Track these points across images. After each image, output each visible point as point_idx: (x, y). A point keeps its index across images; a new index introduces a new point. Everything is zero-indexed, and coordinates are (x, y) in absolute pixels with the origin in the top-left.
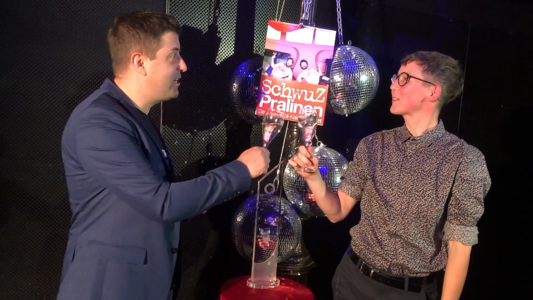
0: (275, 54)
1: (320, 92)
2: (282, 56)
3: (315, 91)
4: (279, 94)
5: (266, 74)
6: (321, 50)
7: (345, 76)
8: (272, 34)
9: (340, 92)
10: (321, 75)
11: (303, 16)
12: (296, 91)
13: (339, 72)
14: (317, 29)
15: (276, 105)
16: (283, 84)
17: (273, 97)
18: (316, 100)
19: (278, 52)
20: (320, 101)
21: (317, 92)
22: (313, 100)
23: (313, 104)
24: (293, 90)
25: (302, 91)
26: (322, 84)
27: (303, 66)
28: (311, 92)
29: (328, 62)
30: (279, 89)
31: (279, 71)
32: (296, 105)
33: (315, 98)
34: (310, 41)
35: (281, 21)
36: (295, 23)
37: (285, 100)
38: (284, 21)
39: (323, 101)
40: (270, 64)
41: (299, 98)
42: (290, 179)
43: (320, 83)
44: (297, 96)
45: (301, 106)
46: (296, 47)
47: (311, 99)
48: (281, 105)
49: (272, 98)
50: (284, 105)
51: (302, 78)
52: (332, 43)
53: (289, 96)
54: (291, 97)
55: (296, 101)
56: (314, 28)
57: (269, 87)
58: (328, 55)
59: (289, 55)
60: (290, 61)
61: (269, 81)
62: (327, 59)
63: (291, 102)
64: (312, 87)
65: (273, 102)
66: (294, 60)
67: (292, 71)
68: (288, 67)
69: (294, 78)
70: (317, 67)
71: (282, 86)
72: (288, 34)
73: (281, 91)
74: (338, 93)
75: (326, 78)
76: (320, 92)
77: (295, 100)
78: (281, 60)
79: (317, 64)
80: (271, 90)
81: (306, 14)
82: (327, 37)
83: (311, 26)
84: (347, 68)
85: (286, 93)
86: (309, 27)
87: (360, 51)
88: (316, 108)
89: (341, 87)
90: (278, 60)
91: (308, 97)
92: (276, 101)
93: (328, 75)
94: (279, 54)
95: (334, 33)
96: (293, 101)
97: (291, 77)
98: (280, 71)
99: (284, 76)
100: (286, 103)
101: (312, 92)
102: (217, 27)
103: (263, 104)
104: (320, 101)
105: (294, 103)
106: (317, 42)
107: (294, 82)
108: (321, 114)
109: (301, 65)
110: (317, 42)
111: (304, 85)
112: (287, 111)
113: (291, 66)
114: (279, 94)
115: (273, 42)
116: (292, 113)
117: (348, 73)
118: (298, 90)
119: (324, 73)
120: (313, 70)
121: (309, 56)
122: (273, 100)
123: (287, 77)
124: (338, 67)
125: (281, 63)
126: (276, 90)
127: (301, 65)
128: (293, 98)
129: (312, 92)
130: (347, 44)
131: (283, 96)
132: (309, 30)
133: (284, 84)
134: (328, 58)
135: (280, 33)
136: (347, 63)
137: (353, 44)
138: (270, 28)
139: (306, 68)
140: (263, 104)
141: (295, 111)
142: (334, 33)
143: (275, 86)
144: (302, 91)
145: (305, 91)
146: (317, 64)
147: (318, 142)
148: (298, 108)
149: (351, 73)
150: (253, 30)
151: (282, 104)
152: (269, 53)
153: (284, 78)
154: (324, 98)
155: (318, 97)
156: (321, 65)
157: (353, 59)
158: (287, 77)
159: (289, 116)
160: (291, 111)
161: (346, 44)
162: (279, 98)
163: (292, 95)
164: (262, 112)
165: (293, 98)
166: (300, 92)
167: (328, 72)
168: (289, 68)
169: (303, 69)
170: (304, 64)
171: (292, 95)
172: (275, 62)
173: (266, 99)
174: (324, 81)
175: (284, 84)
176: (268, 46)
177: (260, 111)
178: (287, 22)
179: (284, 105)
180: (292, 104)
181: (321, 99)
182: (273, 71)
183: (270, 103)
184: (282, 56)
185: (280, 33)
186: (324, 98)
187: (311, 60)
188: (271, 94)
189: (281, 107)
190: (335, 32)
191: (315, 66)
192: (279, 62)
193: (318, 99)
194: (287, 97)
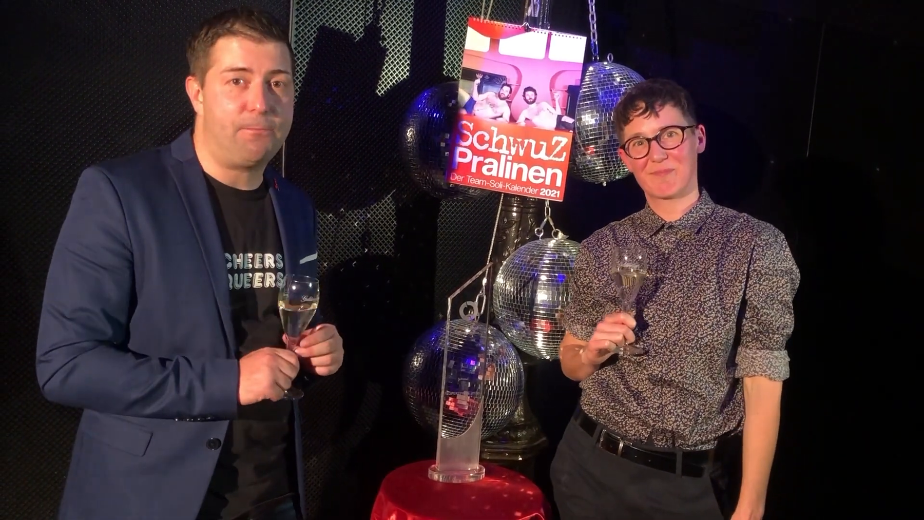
0: (480, 76)
1: (558, 143)
2: (492, 80)
3: (549, 142)
4: (485, 146)
5: (464, 112)
6: (562, 68)
7: (601, 116)
8: (475, 41)
9: (592, 144)
10: (560, 114)
11: (529, 11)
12: (515, 141)
13: (591, 108)
14: (554, 33)
15: (480, 165)
16: (493, 128)
17: (476, 152)
18: (551, 158)
19: (484, 74)
20: (557, 159)
22: (546, 158)
23: (545, 165)
24: (511, 139)
25: (526, 141)
27: (527, 98)
28: (541, 143)
29: (573, 91)
30: (487, 138)
31: (486, 107)
32: (516, 166)
33: (548, 153)
34: (541, 55)
35: (491, 19)
36: (515, 23)
37: (497, 156)
38: (497, 20)
39: (562, 159)
40: (471, 94)
41: (521, 153)
42: (505, 295)
43: (557, 128)
45: (524, 167)
46: (516, 63)
47: (542, 155)
48: (490, 166)
52: (580, 58)
53: (504, 150)
54: (507, 152)
55: (517, 159)
56: (547, 32)
57: (468, 133)
59: (504, 78)
60: (506, 89)
62: (570, 87)
63: (507, 160)
64: (545, 135)
65: (476, 159)
66: (513, 87)
68: (502, 99)
69: (513, 119)
70: (554, 100)
71: (491, 134)
72: (502, 41)
73: (490, 142)
74: (588, 145)
75: (567, 119)
76: (558, 143)
78: (490, 87)
80: (473, 140)
81: (535, 6)
82: (571, 47)
83: (543, 27)
84: (604, 102)
85: (499, 145)
86: (540, 30)
87: (628, 71)
88: (550, 171)
89: (595, 134)
91: (537, 151)
92: (481, 159)
93: (571, 114)
94: (487, 77)
95: (582, 41)
96: (510, 158)
97: (507, 116)
100: (499, 161)
101: (545, 144)
102: (379, 30)
104: (557, 159)
105: (512, 162)
106: (553, 56)
107: (512, 125)
108: (559, 183)
109: (524, 96)
110: (553, 56)
111: (531, 130)
112: (501, 175)
114: (485, 146)
115: (477, 55)
117: (607, 110)
118: (519, 140)
119: (566, 110)
120: (546, 105)
122: (475, 157)
123: (501, 116)
124: (589, 99)
125: (490, 93)
126: (481, 140)
127: (524, 96)
128: (510, 154)
129: (545, 144)
131: (493, 149)
132: (538, 36)
133: (495, 129)
134: (573, 84)
135: (488, 40)
136: (606, 93)
137: (614, 61)
138: (471, 32)
139: (534, 102)
141: (514, 177)
142: (582, 41)
144: (526, 141)
145: (532, 141)
146: (552, 95)
147: (554, 230)
148: (520, 171)
150: (443, 34)
151: (491, 163)
152: (470, 75)
153: (495, 118)
154: (565, 154)
155: (555, 152)
156: (559, 96)
157: (616, 87)
158: (501, 116)
160: (507, 176)
161: (603, 59)
162: (486, 154)
163: (508, 148)
164: (457, 177)
165: (510, 154)
167: (572, 108)
168: (504, 102)
170: (530, 94)
172: (480, 91)
173: (463, 155)
175: (495, 129)
176: (467, 63)
177: (454, 176)
178: (501, 21)
180: (509, 164)
181: (559, 155)
182: (476, 108)
183: (471, 162)
184: (492, 80)
185: (488, 40)
186: (565, 154)
187: (542, 88)
188: (471, 147)
189: (490, 170)
190: (584, 39)
191: (550, 98)
192: (486, 91)
193: (555, 156)
194: (501, 151)
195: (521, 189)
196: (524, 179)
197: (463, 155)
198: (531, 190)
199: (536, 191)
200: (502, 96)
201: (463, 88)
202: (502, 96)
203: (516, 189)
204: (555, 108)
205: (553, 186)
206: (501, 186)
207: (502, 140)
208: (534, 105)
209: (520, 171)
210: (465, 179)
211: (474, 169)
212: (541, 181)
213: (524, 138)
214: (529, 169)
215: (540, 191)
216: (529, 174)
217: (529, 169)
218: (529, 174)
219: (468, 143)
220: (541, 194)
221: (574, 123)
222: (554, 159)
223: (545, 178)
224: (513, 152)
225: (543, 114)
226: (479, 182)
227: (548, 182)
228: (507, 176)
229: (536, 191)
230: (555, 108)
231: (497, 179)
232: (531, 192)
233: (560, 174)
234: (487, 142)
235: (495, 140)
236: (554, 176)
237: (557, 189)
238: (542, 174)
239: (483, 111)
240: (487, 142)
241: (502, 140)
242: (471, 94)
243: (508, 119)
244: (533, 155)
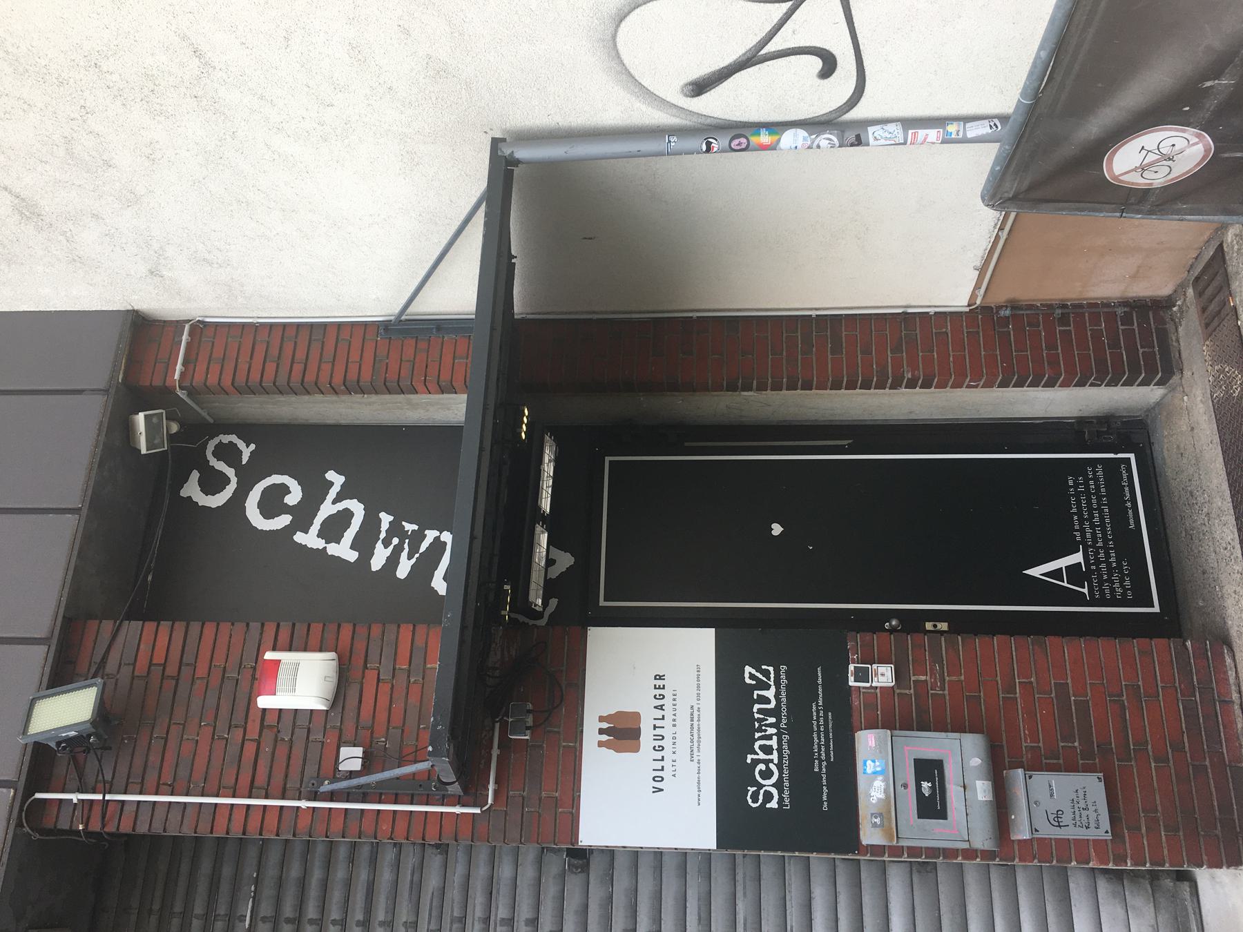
1: (752, 676)
12: (760, 730)
18: (772, 683)
20: (772, 676)
22: (773, 689)
24: (757, 735)
25: (757, 716)
30: (762, 767)
33: (768, 687)
39: (771, 669)
41: (772, 720)
44: (771, 725)
54: (775, 738)
71: (756, 762)
73: (767, 762)
76: (752, 676)
91: (768, 701)
104: (772, 676)
118: (757, 725)
144: (757, 716)
145: (755, 710)
163: (769, 737)
166: (759, 720)
171: (769, 737)
207: (761, 747)
219: (774, 791)
224: (774, 731)
234: (767, 767)
235: (762, 756)
240: (767, 767)
241: (761, 747)
244: (772, 705)
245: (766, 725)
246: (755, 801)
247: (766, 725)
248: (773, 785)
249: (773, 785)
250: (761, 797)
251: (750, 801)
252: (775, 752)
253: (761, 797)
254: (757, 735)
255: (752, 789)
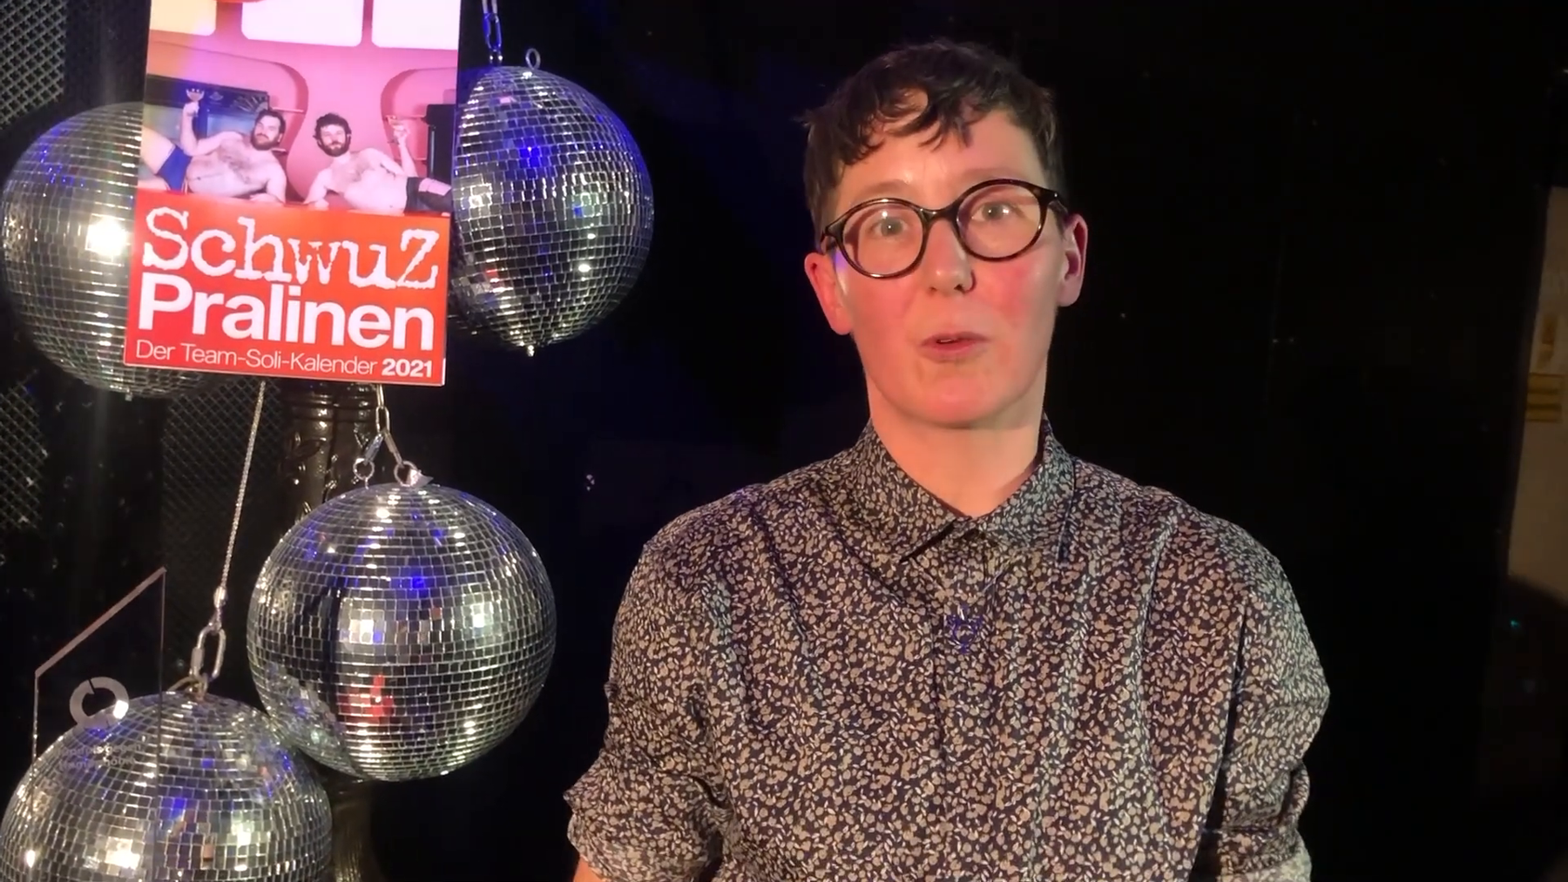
0: (196, 96)
1: (415, 244)
2: (227, 102)
3: (392, 243)
4: (227, 267)
5: (160, 185)
12: (305, 250)
15: (216, 314)
16: (242, 221)
17: (201, 283)
18: (402, 282)
19: (208, 89)
20: (416, 285)
21: (404, 246)
22: (388, 284)
23: (390, 301)
24: (295, 244)
25: (334, 246)
26: (423, 213)
27: (327, 141)
28: (374, 247)
29: (440, 120)
30: (229, 245)
33: (392, 273)
34: (353, 37)
37: (261, 290)
40: (175, 139)
41: (325, 276)
43: (410, 209)
44: (313, 273)
45: (336, 310)
47: (379, 277)
49: (194, 291)
50: (257, 315)
51: (330, 192)
53: (277, 273)
54: (287, 277)
55: (314, 291)
57: (177, 238)
58: (441, 89)
59: (262, 97)
60: (269, 122)
61: (175, 214)
62: (430, 107)
63: (287, 297)
65: (203, 302)
66: (288, 118)
67: (284, 165)
69: (294, 195)
70: (394, 142)
71: (239, 234)
73: (238, 256)
76: (415, 244)
77: (304, 287)
78: (226, 121)
79: (389, 131)
85: (264, 259)
88: (402, 316)
90: (211, 120)
91: (365, 270)
92: (218, 298)
93: (442, 174)
96: (295, 291)
98: (226, 166)
99: (242, 188)
101: (383, 250)
103: (158, 315)
104: (416, 285)
107: (294, 211)
108: (427, 343)
109: (318, 136)
111: (343, 218)
112: (275, 335)
113: (275, 144)
114: (227, 267)
115: (181, 43)
116: (300, 346)
118: (316, 245)
119: (427, 163)
120: (376, 157)
121: (357, 100)
123: (263, 190)
125: (229, 135)
127: (318, 136)
128: (295, 282)
130: (524, 65)
131: (249, 273)
133: (249, 224)
134: (438, 100)
137: (543, 67)
139: (344, 149)
140: (158, 315)
141: (310, 336)
143: (208, 234)
144: (334, 246)
145: (347, 244)
146: (389, 131)
148: (325, 321)
149: (541, 174)
151: (245, 308)
152: (171, 93)
153: (246, 196)
154: (435, 270)
155: (410, 268)
156: (407, 132)
158: (263, 190)
159: (286, 356)
160: (292, 336)
162: (229, 285)
163: (289, 266)
164: (154, 351)
165: (295, 282)
166: (325, 251)
167: (440, 161)
168: (267, 155)
169: (323, 147)
170: (333, 132)
172: (200, 129)
174: (427, 197)
175: (249, 224)
177: (145, 349)
179: (257, 315)
180: (294, 307)
181: (421, 273)
182: (193, 172)
183: (189, 312)
184: (227, 102)
186: (435, 270)
187: (362, 111)
188: (188, 271)
192: (216, 131)
193: (410, 277)
194: (269, 276)
195: (332, 364)
196: (337, 338)
197: (165, 293)
198: (357, 367)
199: (370, 366)
200: (261, 141)
201: (152, 127)
202: (261, 141)
203: (317, 367)
204: (398, 161)
205: (413, 349)
206: (276, 361)
208: (344, 159)
209: (325, 321)
210: (178, 356)
211: (199, 327)
212: (380, 340)
213: (327, 241)
214: (348, 313)
215: (380, 367)
216: (348, 325)
217: (348, 313)
218: (348, 325)
219: (178, 262)
220: (386, 372)
221: (450, 192)
222: (409, 284)
223: (390, 333)
224: (302, 272)
225: (371, 178)
226: (216, 357)
227: (399, 342)
228: (292, 336)
229: (370, 366)
230: (398, 161)
231: (266, 345)
232: (357, 370)
233: (427, 319)
234: (228, 256)
235: (251, 248)
236: (414, 327)
237: (425, 356)
238: (383, 322)
239: (213, 180)
240: (228, 256)
242: (175, 139)
243: (282, 197)
244: (355, 279)
245: (314, 265)
246: (162, 222)
247: (314, 265)
248: (190, 263)
249: (190, 263)
250: (166, 235)
251: (160, 211)
252: (256, 275)
253: (166, 235)
254: (295, 244)
255: (183, 219)
